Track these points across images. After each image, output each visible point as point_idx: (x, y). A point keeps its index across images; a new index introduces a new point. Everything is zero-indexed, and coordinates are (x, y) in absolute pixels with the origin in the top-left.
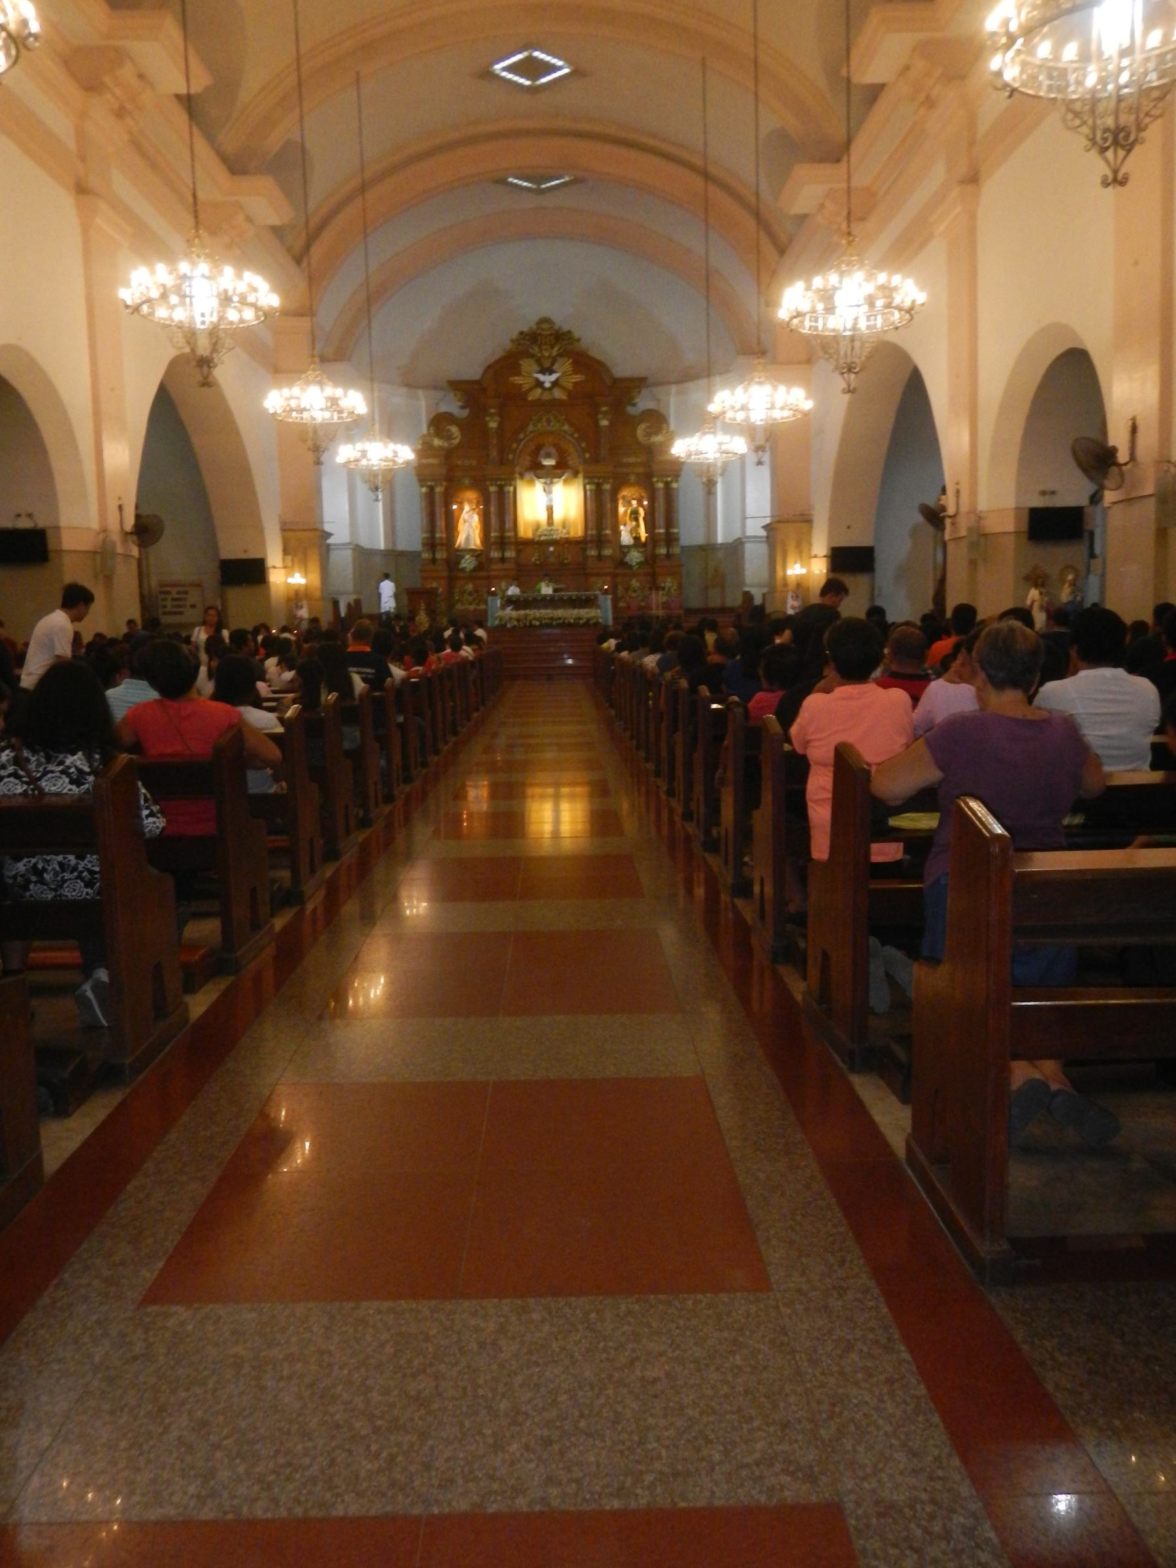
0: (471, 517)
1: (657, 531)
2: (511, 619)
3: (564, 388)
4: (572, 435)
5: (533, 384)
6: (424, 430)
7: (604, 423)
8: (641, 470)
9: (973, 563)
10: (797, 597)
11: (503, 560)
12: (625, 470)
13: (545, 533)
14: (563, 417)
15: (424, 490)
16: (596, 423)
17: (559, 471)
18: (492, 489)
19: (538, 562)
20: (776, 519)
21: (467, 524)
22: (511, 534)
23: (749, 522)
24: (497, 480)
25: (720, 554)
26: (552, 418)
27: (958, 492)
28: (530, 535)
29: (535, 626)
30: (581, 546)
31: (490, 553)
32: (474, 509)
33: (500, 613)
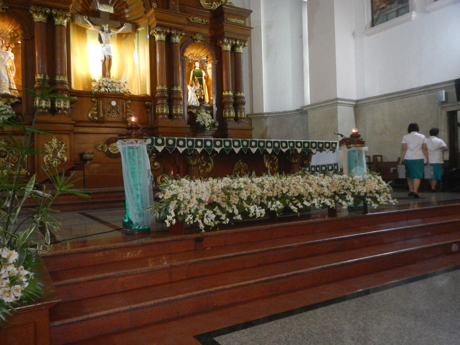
1: (226, 93)
12: (194, 29)
13: (105, 84)
18: (38, 18)
19: (96, 118)
24: (44, 6)
25: (268, 122)
28: (81, 89)
30: (146, 103)
31: (33, 100)
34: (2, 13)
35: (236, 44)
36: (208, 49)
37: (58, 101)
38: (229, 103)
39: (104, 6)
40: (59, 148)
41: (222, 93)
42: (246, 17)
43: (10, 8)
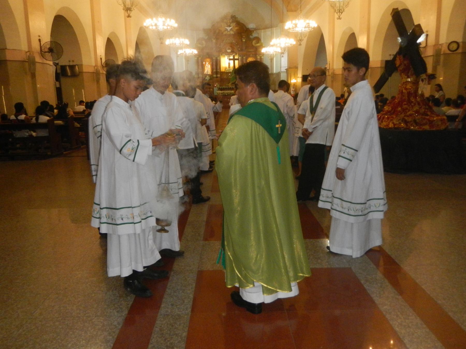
0: (208, 66)
2: (220, 93)
3: (233, 31)
4: (235, 44)
6: (196, 43)
7: (244, 40)
8: (253, 53)
9: (332, 81)
10: (294, 88)
11: (217, 77)
13: (228, 70)
15: (196, 58)
16: (242, 40)
17: (232, 53)
20: (289, 67)
21: (207, 68)
22: (219, 70)
23: (282, 68)
25: (274, 76)
27: (330, 64)
28: (224, 70)
29: (226, 95)
32: (209, 64)
33: (217, 92)
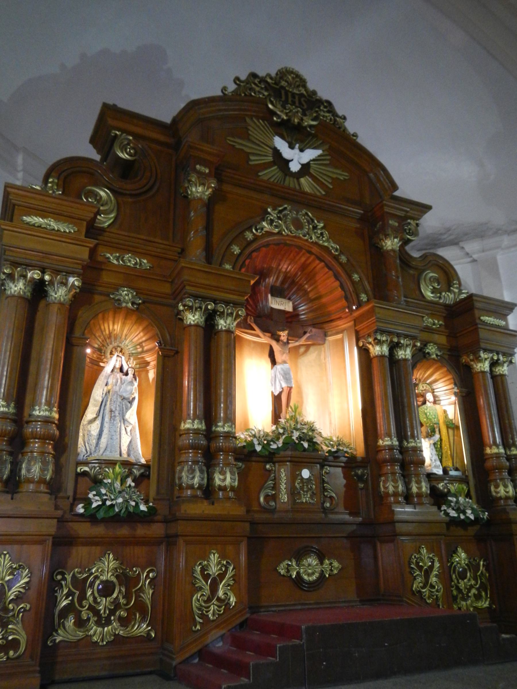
5: (271, 159)
14: (322, 225)
26: (303, 220)
34: (131, 310)
35: (498, 359)
36: (448, 370)
37: (220, 473)
38: (500, 469)
39: (279, 300)
40: (222, 576)
41: (377, 442)
42: (508, 315)
43: (144, 302)
